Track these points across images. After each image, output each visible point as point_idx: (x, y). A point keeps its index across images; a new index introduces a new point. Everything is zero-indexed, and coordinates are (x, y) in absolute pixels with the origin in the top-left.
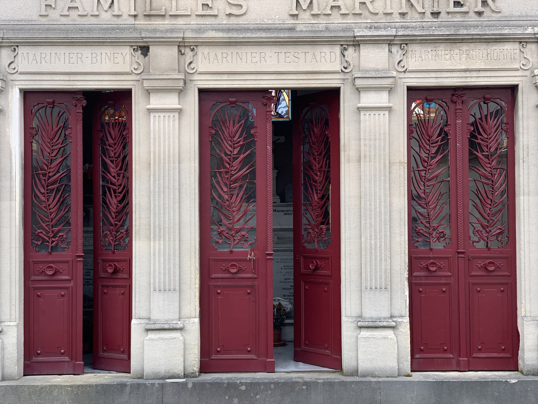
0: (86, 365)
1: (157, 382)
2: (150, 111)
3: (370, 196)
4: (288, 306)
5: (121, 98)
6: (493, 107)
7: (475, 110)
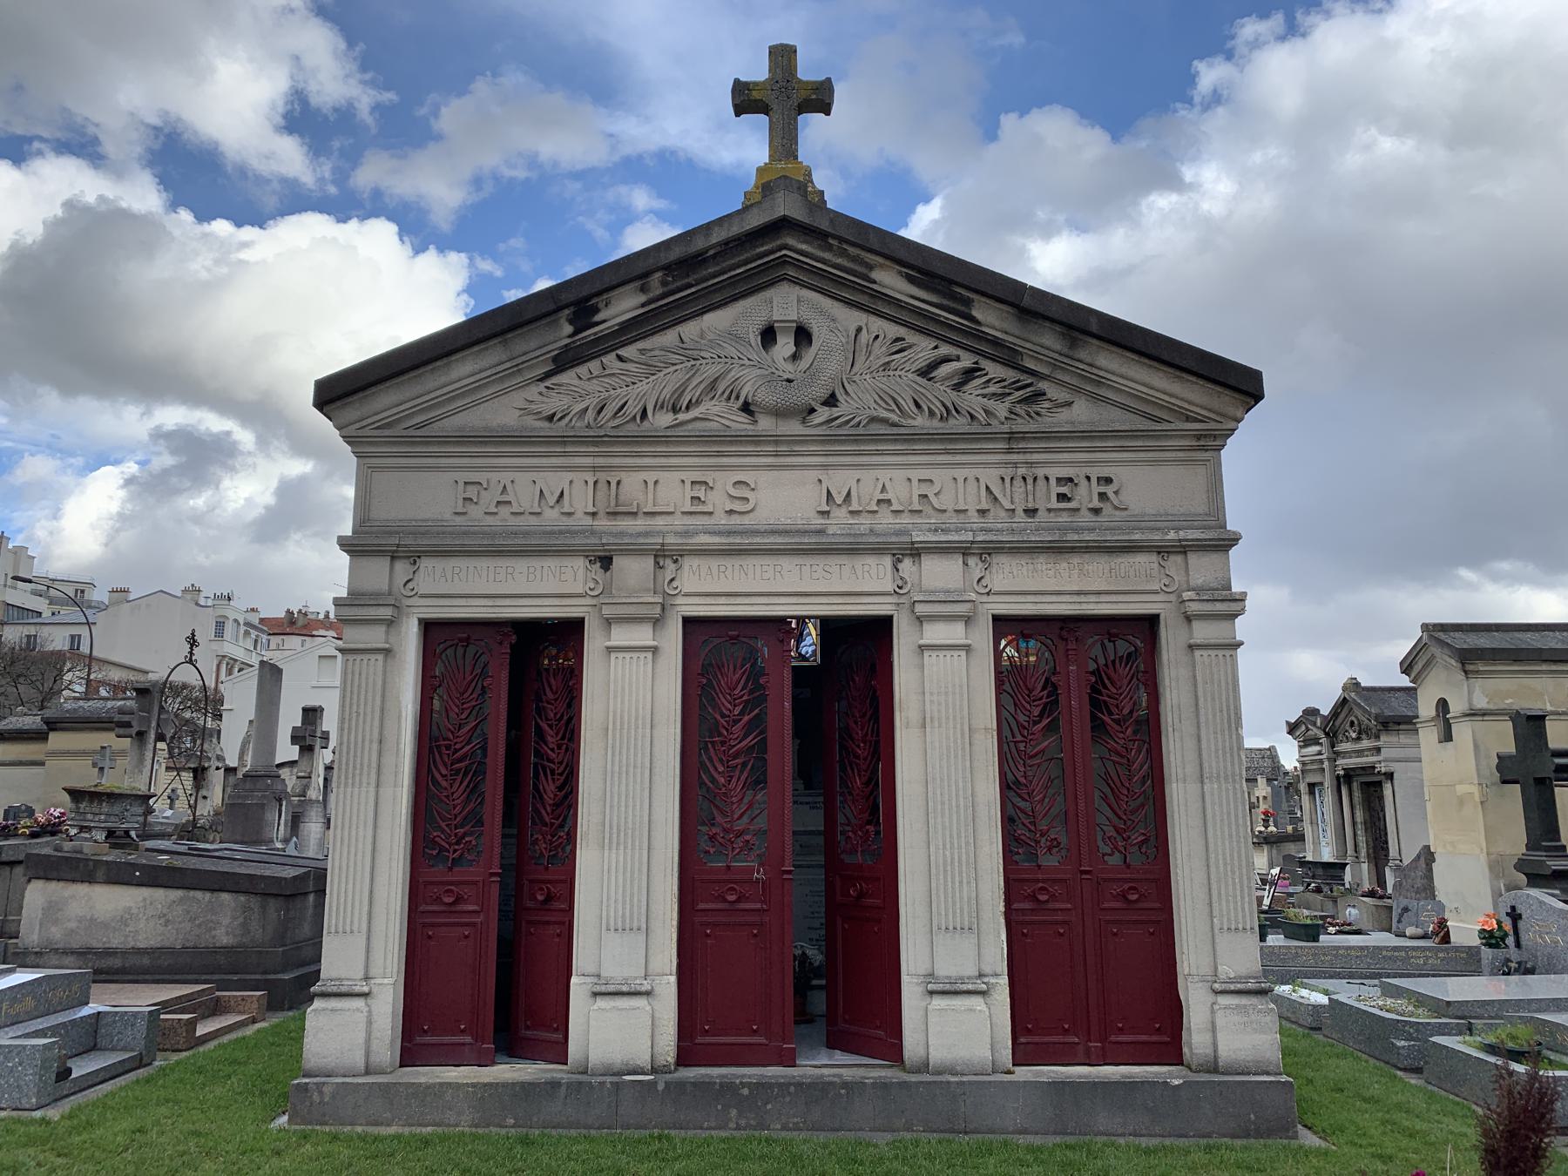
0: (497, 1050)
1: (609, 1079)
2: (610, 650)
3: (942, 780)
4: (816, 956)
5: (569, 632)
6: (1123, 648)
7: (1097, 651)
